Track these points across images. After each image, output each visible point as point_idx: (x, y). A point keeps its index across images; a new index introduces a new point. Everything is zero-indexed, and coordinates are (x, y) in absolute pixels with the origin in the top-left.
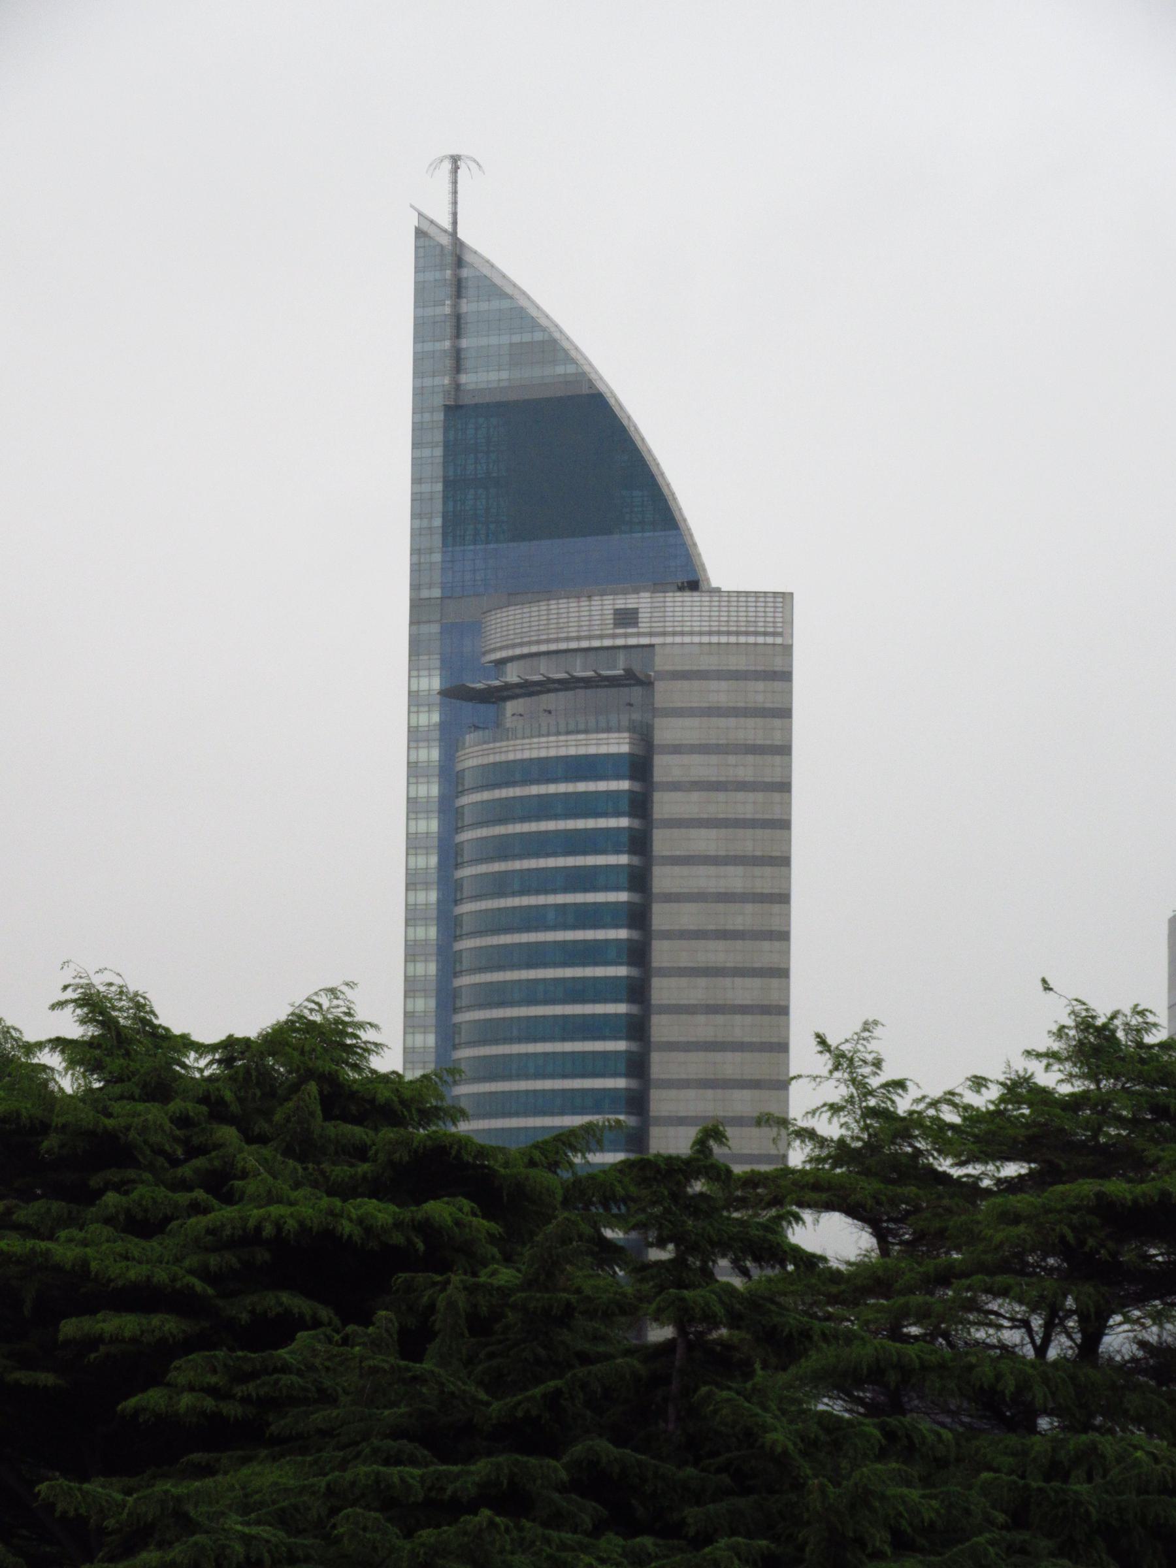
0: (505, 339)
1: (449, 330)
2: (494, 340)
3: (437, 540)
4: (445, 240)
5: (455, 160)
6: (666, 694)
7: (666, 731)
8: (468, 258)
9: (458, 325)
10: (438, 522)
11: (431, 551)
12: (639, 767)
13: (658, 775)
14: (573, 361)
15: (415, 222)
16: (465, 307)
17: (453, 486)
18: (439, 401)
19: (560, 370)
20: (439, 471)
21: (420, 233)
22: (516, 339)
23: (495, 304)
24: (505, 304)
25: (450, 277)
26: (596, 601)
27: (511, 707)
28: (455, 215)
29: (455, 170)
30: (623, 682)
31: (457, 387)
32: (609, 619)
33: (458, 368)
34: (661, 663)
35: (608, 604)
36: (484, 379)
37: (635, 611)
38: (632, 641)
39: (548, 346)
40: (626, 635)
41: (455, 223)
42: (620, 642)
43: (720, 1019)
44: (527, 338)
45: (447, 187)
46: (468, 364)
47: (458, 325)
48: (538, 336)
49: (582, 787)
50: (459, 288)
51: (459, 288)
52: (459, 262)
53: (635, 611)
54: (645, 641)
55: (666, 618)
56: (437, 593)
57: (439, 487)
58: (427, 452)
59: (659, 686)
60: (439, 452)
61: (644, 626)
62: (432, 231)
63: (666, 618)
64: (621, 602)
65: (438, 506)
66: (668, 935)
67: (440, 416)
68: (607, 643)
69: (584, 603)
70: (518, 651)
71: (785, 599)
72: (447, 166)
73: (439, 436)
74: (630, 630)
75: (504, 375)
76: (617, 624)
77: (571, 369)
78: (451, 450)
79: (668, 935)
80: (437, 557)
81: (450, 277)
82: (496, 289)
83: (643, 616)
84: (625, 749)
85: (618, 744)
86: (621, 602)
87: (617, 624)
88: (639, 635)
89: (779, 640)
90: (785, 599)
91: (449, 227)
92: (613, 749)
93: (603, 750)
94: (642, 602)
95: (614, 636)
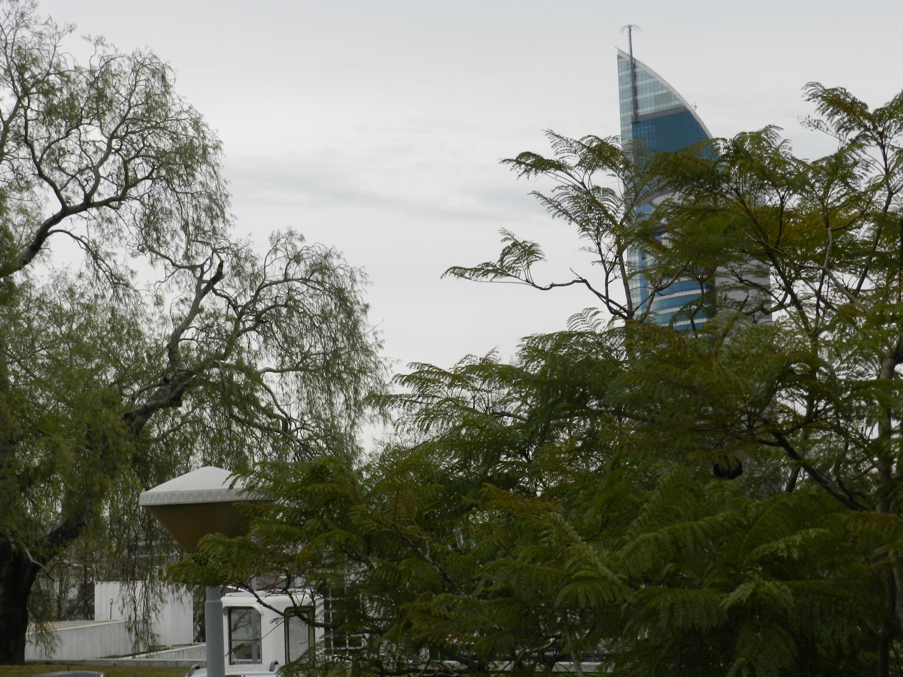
0: (653, 94)
2: (648, 95)
4: (628, 59)
5: (630, 27)
8: (637, 64)
14: (678, 99)
15: (616, 53)
18: (630, 121)
19: (673, 103)
21: (619, 57)
22: (656, 93)
23: (648, 81)
25: (631, 70)
29: (630, 31)
39: (670, 95)
44: (660, 92)
46: (640, 105)
48: (664, 91)
50: (634, 76)
51: (634, 76)
62: (623, 55)
67: (631, 127)
77: (677, 103)
81: (631, 70)
82: (649, 75)
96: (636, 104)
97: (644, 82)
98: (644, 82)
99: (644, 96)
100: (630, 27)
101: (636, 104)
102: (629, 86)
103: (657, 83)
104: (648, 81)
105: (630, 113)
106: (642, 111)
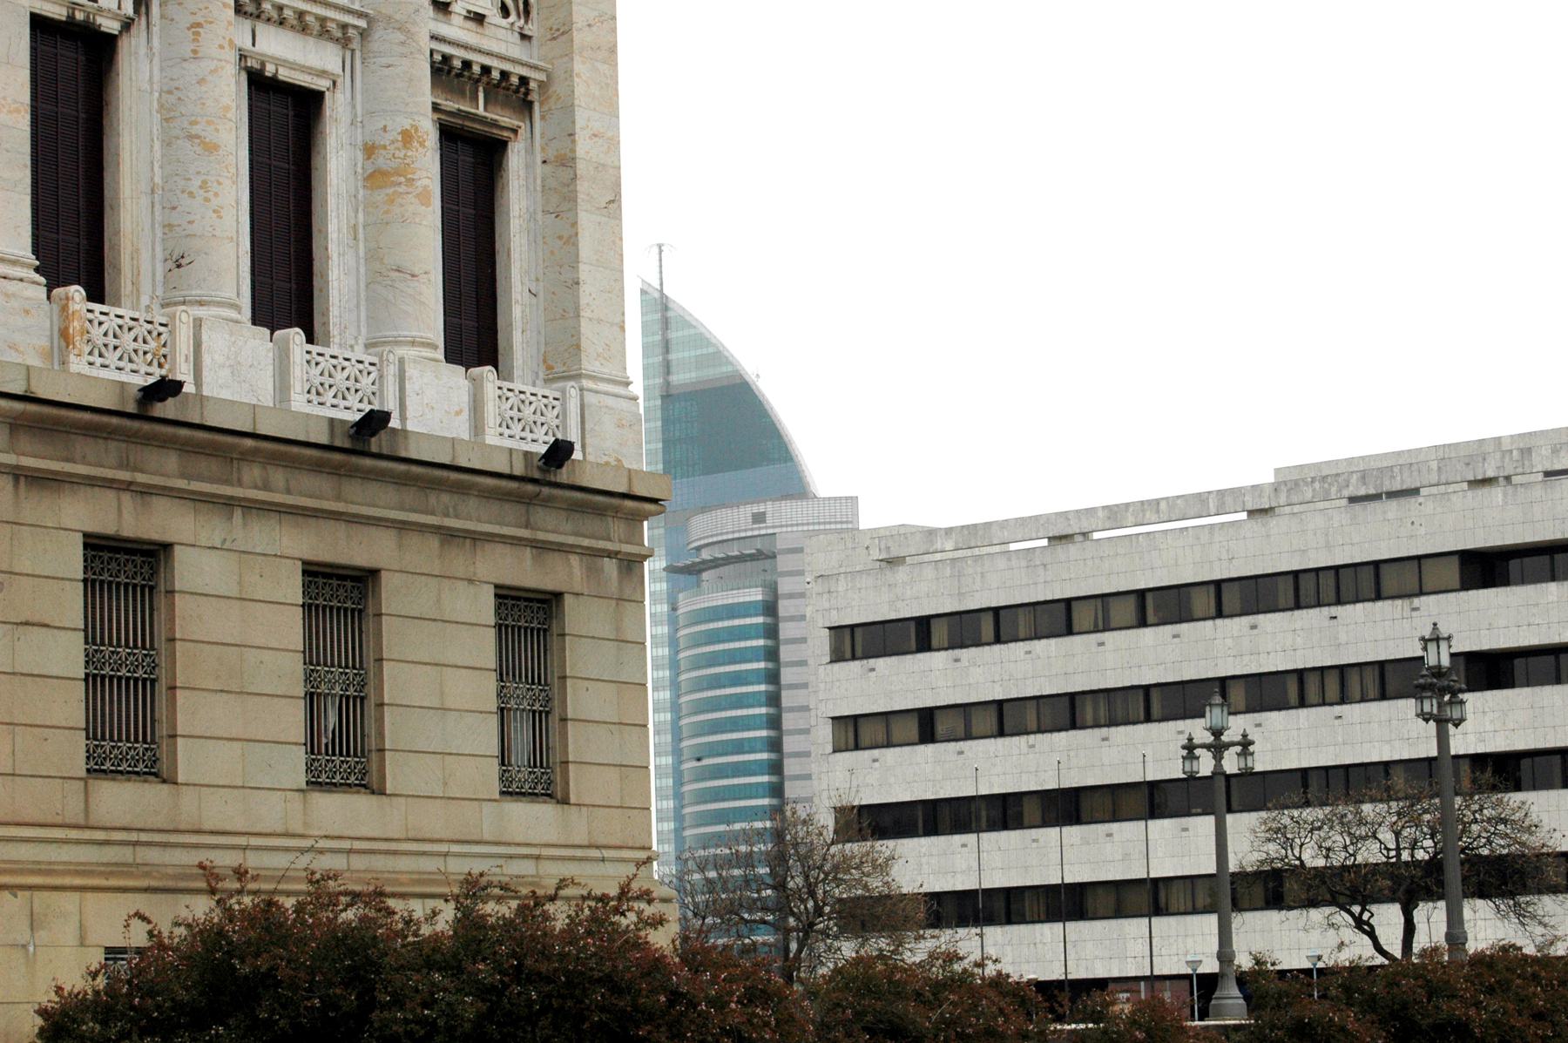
0: (693, 353)
1: (659, 350)
2: (686, 354)
4: (657, 295)
5: (660, 246)
6: (783, 563)
7: (785, 586)
8: (671, 305)
9: (666, 347)
12: (770, 608)
13: (782, 612)
15: (640, 285)
16: (672, 335)
18: (657, 393)
19: (724, 369)
20: (660, 436)
21: (643, 292)
22: (699, 352)
23: (686, 332)
24: (692, 331)
26: (742, 509)
27: (705, 575)
29: (661, 252)
30: (758, 557)
31: (667, 384)
34: (780, 545)
35: (748, 511)
36: (679, 378)
37: (764, 514)
39: (718, 356)
44: (705, 351)
46: (673, 369)
47: (666, 347)
48: (711, 350)
49: (737, 622)
50: (666, 323)
51: (666, 323)
52: (666, 308)
53: (764, 514)
54: (770, 531)
55: (783, 516)
60: (659, 423)
61: (769, 522)
62: (650, 290)
63: (783, 516)
64: (756, 509)
67: (659, 402)
71: (853, 501)
72: (656, 250)
73: (659, 414)
75: (694, 375)
76: (754, 522)
77: (730, 369)
78: (666, 422)
79: (792, 709)
82: (687, 323)
84: (760, 598)
85: (756, 595)
86: (756, 509)
87: (754, 522)
90: (853, 501)
92: (753, 598)
93: (748, 599)
94: (768, 507)
96: (667, 368)
97: (680, 334)
98: (680, 334)
99: (680, 355)
100: (660, 246)
101: (667, 368)
102: (658, 338)
103: (701, 339)
104: (686, 332)
105: (659, 381)
106: (678, 378)
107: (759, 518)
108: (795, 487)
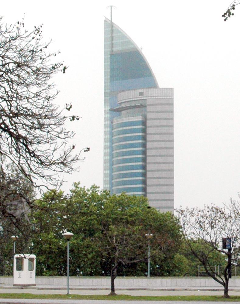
0: (121, 41)
3: (109, 80)
4: (109, 22)
5: (111, 7)
6: (149, 109)
8: (114, 25)
10: (109, 77)
11: (108, 83)
14: (133, 44)
17: (112, 70)
18: (109, 53)
19: (131, 46)
20: (109, 67)
22: (123, 41)
25: (111, 30)
28: (111, 17)
29: (111, 8)
30: (141, 106)
31: (112, 51)
32: (138, 94)
33: (112, 47)
34: (148, 102)
35: (137, 92)
36: (116, 49)
37: (143, 92)
38: (142, 98)
39: (129, 42)
40: (141, 97)
41: (111, 19)
42: (140, 99)
43: (160, 172)
44: (125, 40)
45: (110, 12)
46: (114, 46)
48: (127, 40)
50: (112, 31)
51: (112, 31)
53: (143, 92)
54: (145, 98)
56: (109, 91)
57: (109, 70)
58: (107, 63)
59: (147, 107)
60: (109, 63)
61: (145, 95)
62: (107, 20)
63: (149, 93)
64: (140, 91)
65: (109, 74)
66: (149, 156)
67: (109, 56)
68: (138, 99)
69: (134, 91)
70: (123, 101)
72: (110, 8)
73: (109, 60)
74: (142, 96)
75: (121, 48)
76: (140, 95)
77: (133, 46)
78: (111, 62)
80: (109, 84)
81: (111, 30)
82: (119, 31)
83: (144, 93)
86: (140, 91)
87: (140, 95)
88: (143, 97)
89: (171, 97)
91: (110, 19)
94: (144, 90)
95: (139, 97)
96: (112, 45)
101: (112, 45)
102: (110, 36)
103: (124, 36)
105: (110, 50)
106: (115, 49)
107: (141, 94)
108: (153, 85)
